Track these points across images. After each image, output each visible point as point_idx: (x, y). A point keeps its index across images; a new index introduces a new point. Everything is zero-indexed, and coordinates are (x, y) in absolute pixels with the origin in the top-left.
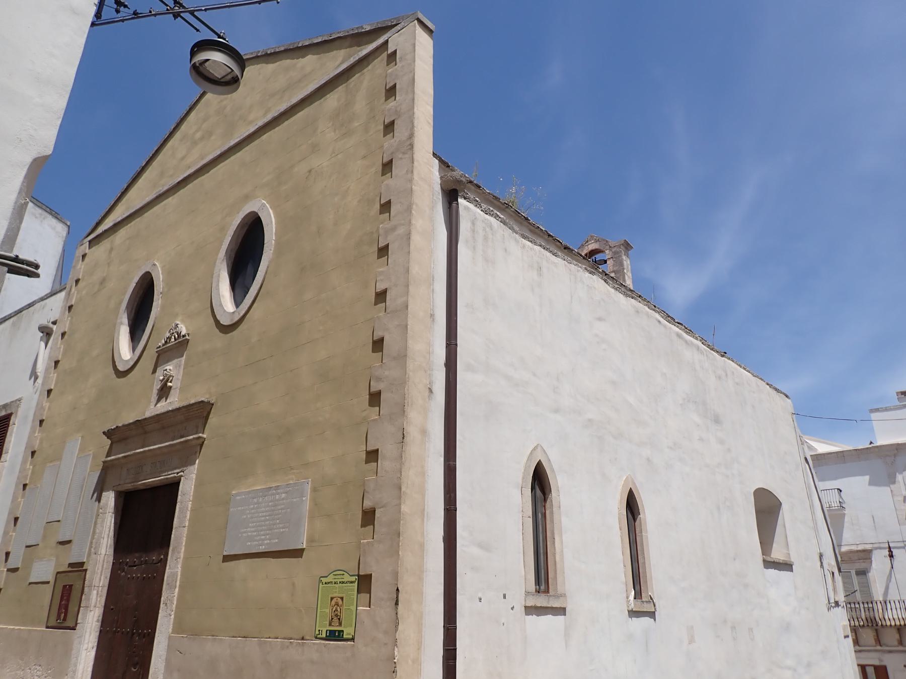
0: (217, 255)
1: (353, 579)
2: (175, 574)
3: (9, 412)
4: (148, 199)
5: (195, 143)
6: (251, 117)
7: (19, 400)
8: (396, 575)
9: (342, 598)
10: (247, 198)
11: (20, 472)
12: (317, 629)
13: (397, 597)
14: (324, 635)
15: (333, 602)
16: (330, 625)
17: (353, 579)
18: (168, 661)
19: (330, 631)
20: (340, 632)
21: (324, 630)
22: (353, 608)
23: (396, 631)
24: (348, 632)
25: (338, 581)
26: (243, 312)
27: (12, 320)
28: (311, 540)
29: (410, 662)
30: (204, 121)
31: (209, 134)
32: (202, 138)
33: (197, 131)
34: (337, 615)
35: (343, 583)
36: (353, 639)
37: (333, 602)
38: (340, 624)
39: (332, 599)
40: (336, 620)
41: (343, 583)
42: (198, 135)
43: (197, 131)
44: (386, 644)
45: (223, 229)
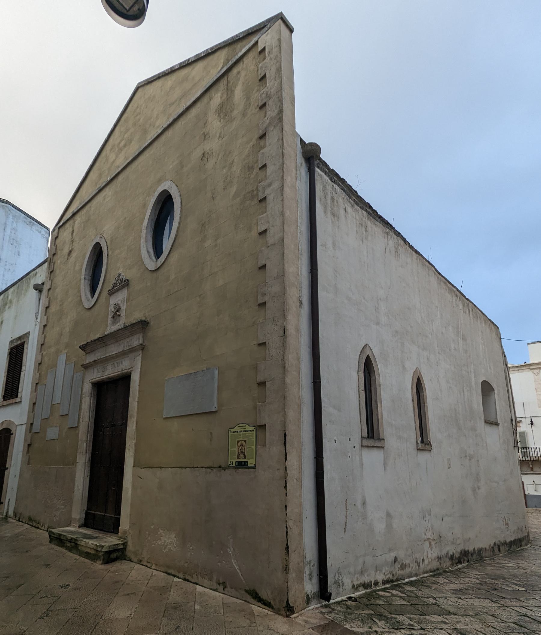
0: (142, 224)
1: (252, 428)
2: (112, 352)
3: (23, 341)
4: (93, 194)
5: (121, 150)
6: (158, 123)
7: (29, 332)
8: (284, 424)
9: (245, 441)
10: (160, 181)
11: (33, 376)
12: (229, 461)
13: (285, 439)
14: (234, 465)
15: (239, 444)
16: (238, 458)
17: (252, 428)
18: (133, 483)
19: (238, 462)
20: (245, 462)
21: (234, 461)
22: (254, 447)
23: (286, 461)
24: (251, 462)
25: (242, 430)
26: (163, 260)
27: (17, 285)
28: (220, 405)
29: (295, 480)
30: (126, 132)
31: (130, 141)
32: (125, 146)
33: (121, 141)
34: (242, 452)
35: (245, 431)
36: (254, 467)
37: (239, 444)
38: (245, 458)
39: (238, 442)
40: (242, 455)
41: (245, 431)
42: (123, 143)
43: (121, 141)
44: (278, 469)
45: (145, 206)
